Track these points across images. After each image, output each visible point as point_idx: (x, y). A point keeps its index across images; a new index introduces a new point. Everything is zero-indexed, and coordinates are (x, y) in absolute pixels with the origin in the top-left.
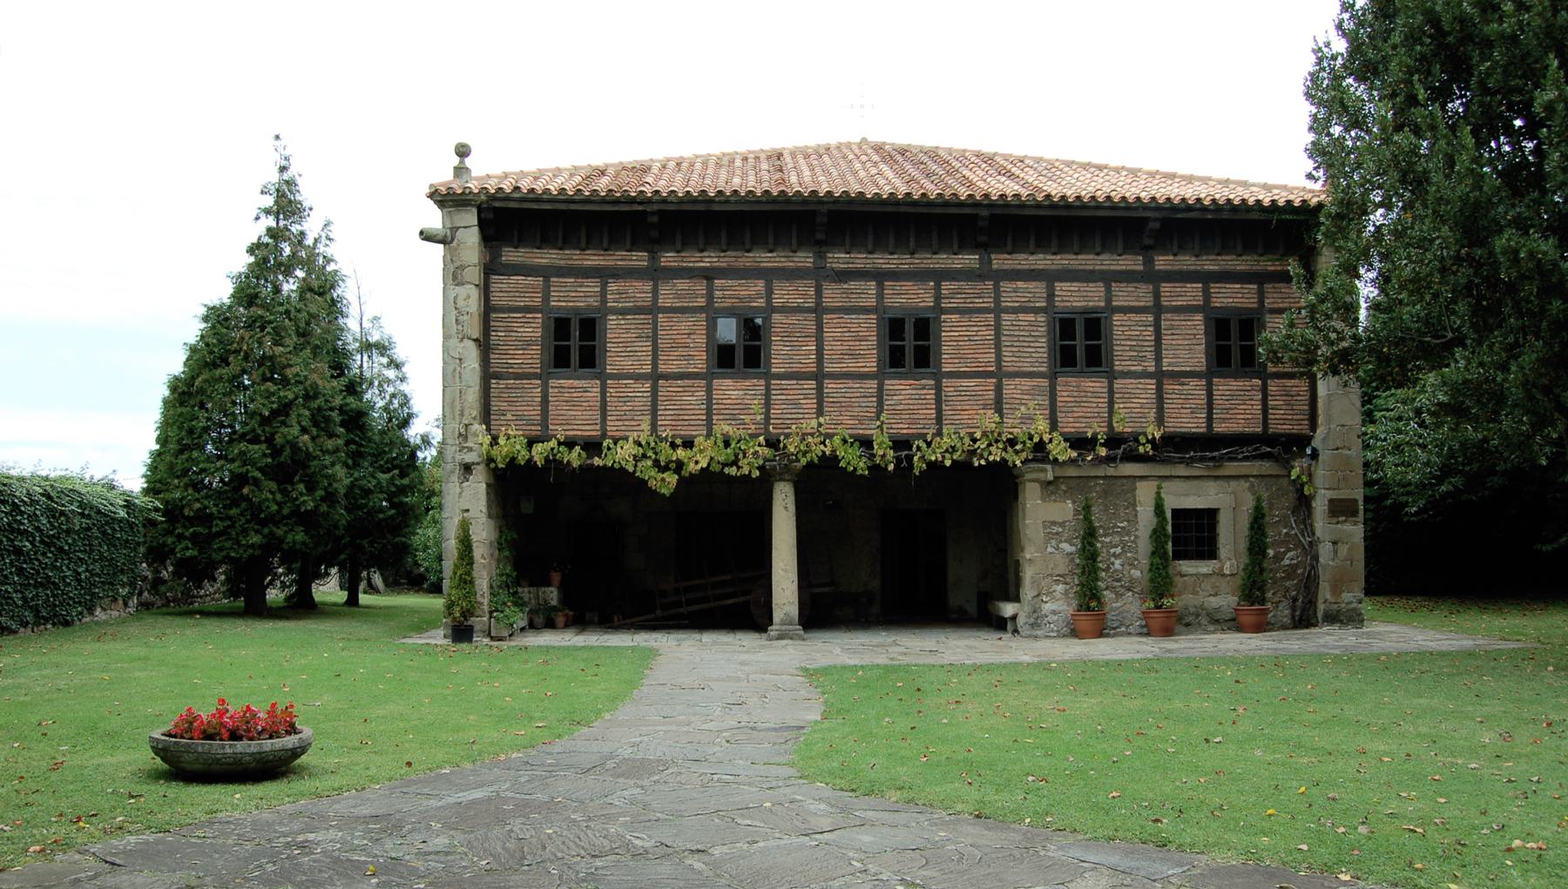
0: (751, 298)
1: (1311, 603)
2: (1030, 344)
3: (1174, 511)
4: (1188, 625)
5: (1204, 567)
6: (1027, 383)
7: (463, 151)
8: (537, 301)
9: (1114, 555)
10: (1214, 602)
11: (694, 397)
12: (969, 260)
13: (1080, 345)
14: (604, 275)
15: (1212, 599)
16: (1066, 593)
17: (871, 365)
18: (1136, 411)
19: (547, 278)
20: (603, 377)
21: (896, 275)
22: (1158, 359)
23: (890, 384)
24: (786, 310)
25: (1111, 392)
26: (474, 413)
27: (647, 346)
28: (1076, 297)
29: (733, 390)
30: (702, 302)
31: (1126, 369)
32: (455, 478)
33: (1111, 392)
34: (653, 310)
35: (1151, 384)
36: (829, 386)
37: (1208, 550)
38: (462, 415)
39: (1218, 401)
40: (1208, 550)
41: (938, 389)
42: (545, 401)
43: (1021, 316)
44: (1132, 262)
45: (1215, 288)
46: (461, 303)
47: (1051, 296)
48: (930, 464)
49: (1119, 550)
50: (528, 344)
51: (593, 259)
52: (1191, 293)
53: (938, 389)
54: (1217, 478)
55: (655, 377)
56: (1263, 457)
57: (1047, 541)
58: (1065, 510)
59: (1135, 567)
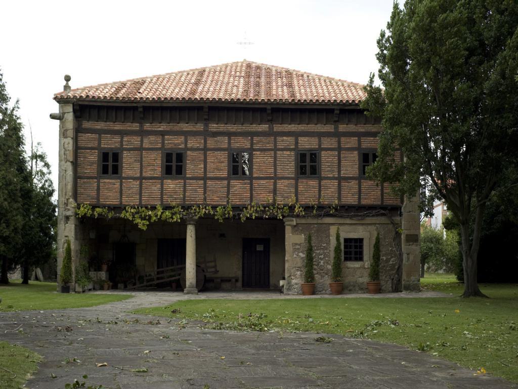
0: (179, 144)
1: (399, 281)
2: (288, 165)
3: (346, 240)
4: (350, 290)
5: (357, 264)
6: (286, 182)
7: (68, 79)
8: (96, 144)
9: (321, 259)
10: (361, 280)
11: (156, 188)
12: (264, 127)
13: (308, 164)
14: (122, 133)
15: (360, 279)
16: (301, 275)
17: (225, 174)
18: (329, 195)
19: (100, 135)
20: (121, 178)
21: (235, 134)
22: (339, 171)
23: (233, 182)
24: (192, 149)
25: (320, 186)
26: (70, 194)
27: (138, 165)
28: (307, 143)
29: (171, 185)
30: (159, 146)
31: (326, 176)
32: (62, 222)
33: (320, 186)
34: (140, 149)
35: (336, 183)
36: (209, 183)
37: (359, 257)
38: (66, 195)
39: (363, 190)
40: (359, 257)
41: (251, 184)
42: (98, 189)
43: (285, 152)
44: (329, 128)
45: (363, 139)
46: (66, 146)
47: (297, 143)
48: (247, 218)
49: (322, 256)
50: (92, 164)
51: (118, 127)
52: (353, 142)
53: (251, 184)
54: (363, 224)
55: (141, 178)
56: (383, 215)
57: (294, 252)
58: (301, 238)
59: (329, 265)
